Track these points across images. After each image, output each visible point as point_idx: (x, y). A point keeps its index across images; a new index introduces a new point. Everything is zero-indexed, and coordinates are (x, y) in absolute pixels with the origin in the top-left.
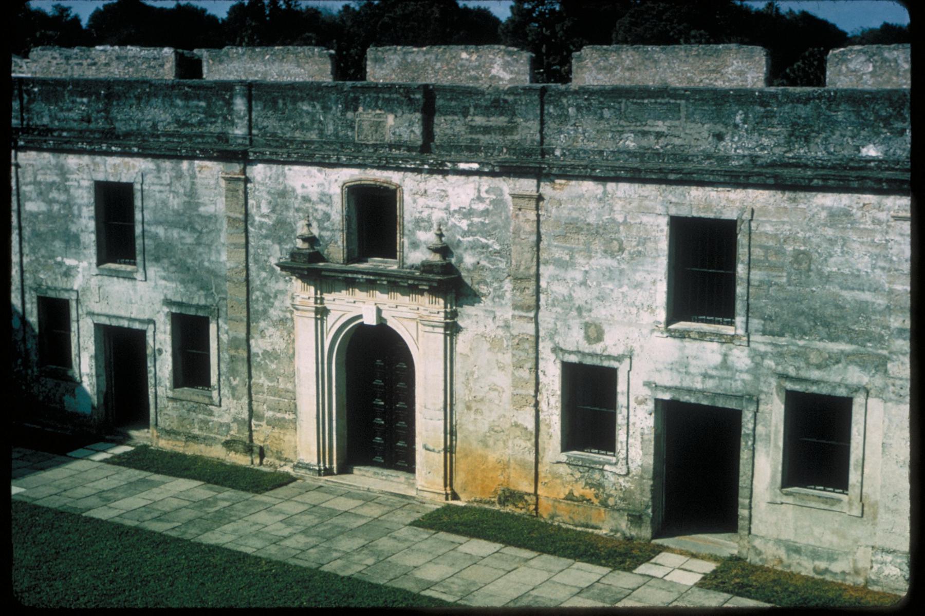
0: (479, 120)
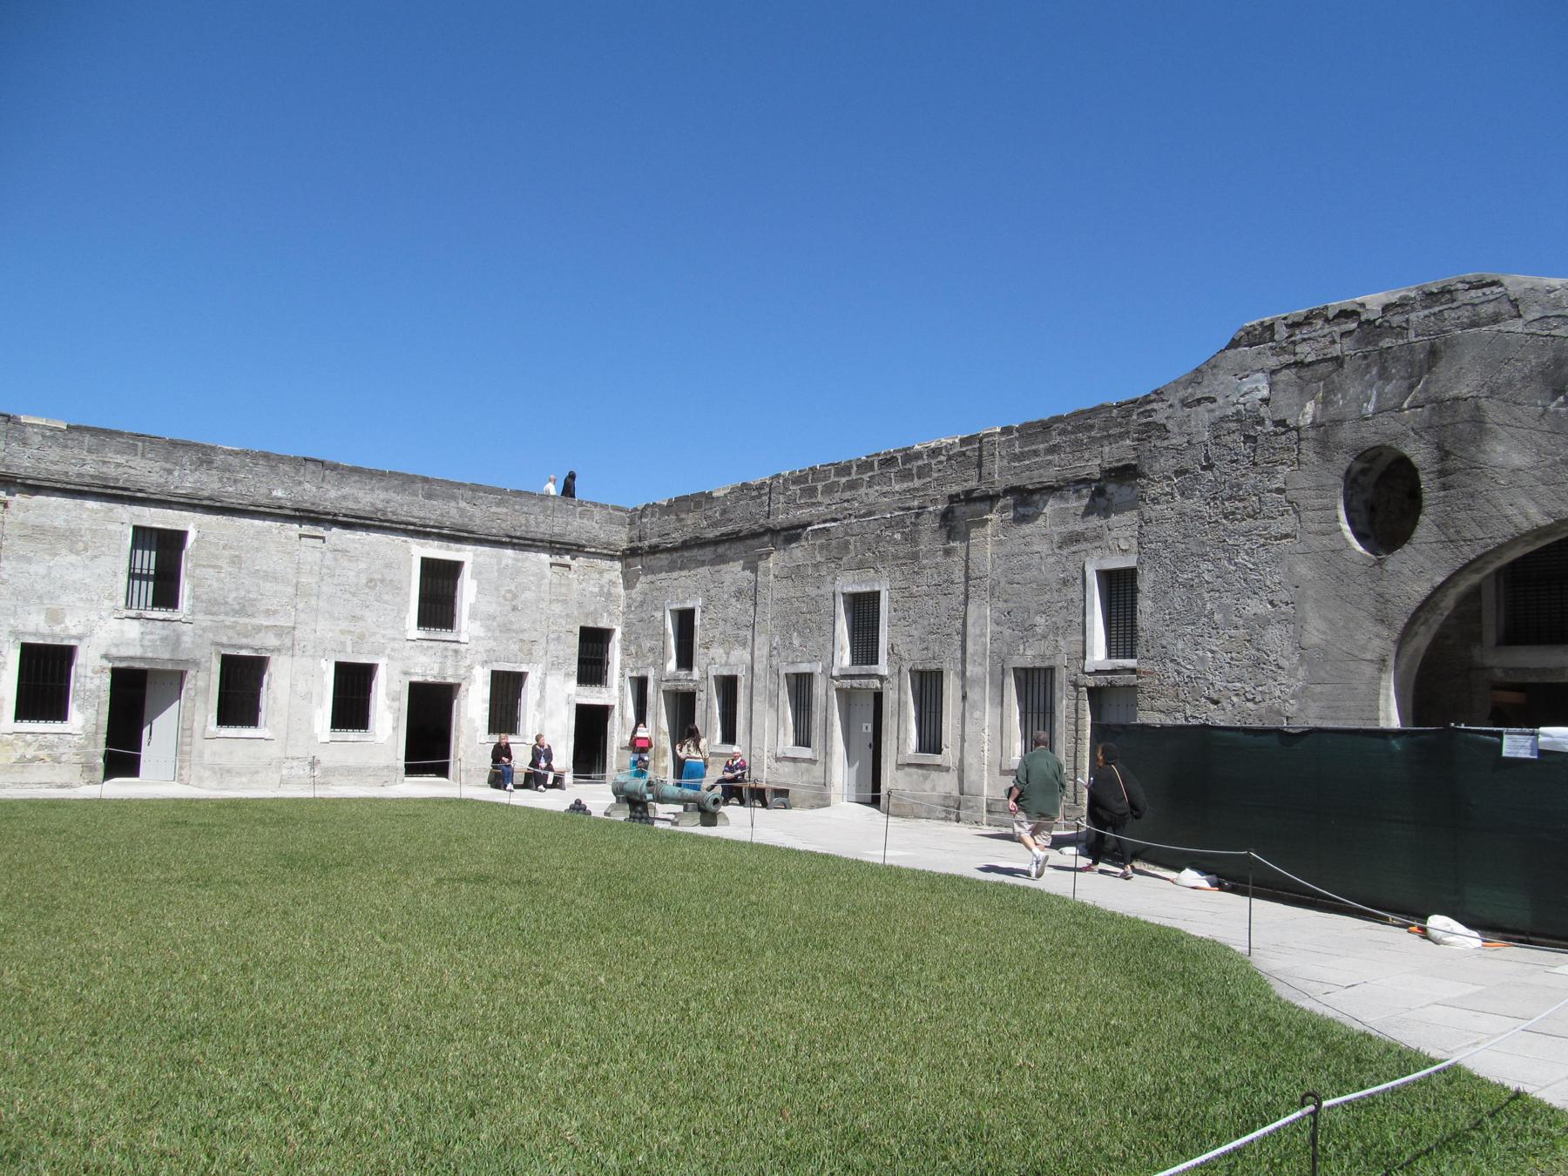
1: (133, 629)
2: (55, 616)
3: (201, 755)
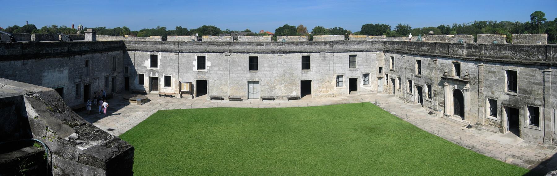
0: (474, 50)
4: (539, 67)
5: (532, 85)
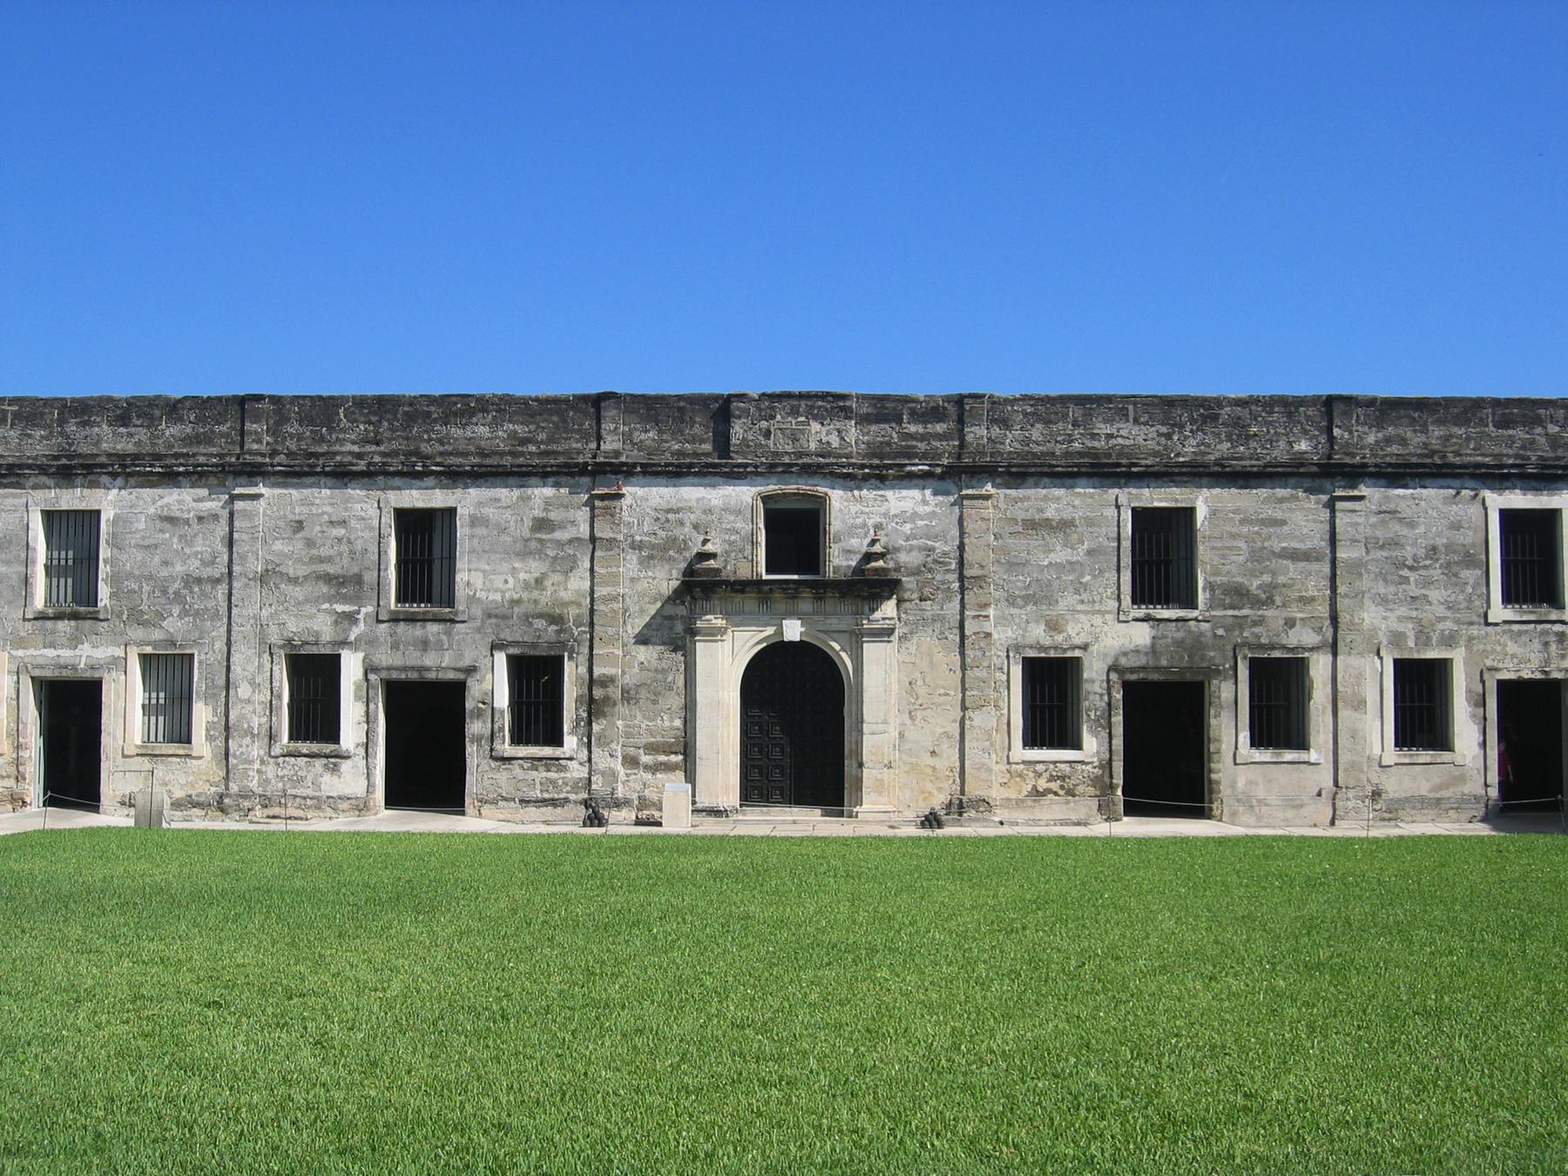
0: (912, 428)
1: (1141, 635)
2: (1053, 626)
3: (1233, 785)
4: (1308, 483)
5: (1274, 564)
